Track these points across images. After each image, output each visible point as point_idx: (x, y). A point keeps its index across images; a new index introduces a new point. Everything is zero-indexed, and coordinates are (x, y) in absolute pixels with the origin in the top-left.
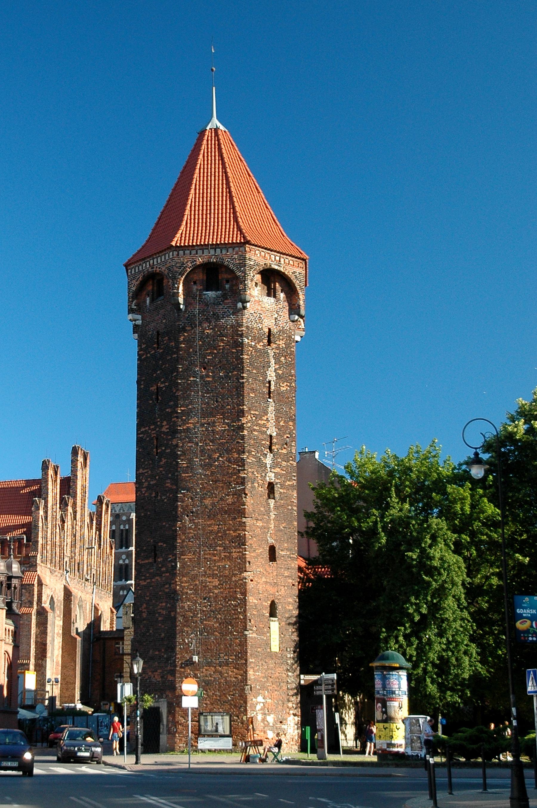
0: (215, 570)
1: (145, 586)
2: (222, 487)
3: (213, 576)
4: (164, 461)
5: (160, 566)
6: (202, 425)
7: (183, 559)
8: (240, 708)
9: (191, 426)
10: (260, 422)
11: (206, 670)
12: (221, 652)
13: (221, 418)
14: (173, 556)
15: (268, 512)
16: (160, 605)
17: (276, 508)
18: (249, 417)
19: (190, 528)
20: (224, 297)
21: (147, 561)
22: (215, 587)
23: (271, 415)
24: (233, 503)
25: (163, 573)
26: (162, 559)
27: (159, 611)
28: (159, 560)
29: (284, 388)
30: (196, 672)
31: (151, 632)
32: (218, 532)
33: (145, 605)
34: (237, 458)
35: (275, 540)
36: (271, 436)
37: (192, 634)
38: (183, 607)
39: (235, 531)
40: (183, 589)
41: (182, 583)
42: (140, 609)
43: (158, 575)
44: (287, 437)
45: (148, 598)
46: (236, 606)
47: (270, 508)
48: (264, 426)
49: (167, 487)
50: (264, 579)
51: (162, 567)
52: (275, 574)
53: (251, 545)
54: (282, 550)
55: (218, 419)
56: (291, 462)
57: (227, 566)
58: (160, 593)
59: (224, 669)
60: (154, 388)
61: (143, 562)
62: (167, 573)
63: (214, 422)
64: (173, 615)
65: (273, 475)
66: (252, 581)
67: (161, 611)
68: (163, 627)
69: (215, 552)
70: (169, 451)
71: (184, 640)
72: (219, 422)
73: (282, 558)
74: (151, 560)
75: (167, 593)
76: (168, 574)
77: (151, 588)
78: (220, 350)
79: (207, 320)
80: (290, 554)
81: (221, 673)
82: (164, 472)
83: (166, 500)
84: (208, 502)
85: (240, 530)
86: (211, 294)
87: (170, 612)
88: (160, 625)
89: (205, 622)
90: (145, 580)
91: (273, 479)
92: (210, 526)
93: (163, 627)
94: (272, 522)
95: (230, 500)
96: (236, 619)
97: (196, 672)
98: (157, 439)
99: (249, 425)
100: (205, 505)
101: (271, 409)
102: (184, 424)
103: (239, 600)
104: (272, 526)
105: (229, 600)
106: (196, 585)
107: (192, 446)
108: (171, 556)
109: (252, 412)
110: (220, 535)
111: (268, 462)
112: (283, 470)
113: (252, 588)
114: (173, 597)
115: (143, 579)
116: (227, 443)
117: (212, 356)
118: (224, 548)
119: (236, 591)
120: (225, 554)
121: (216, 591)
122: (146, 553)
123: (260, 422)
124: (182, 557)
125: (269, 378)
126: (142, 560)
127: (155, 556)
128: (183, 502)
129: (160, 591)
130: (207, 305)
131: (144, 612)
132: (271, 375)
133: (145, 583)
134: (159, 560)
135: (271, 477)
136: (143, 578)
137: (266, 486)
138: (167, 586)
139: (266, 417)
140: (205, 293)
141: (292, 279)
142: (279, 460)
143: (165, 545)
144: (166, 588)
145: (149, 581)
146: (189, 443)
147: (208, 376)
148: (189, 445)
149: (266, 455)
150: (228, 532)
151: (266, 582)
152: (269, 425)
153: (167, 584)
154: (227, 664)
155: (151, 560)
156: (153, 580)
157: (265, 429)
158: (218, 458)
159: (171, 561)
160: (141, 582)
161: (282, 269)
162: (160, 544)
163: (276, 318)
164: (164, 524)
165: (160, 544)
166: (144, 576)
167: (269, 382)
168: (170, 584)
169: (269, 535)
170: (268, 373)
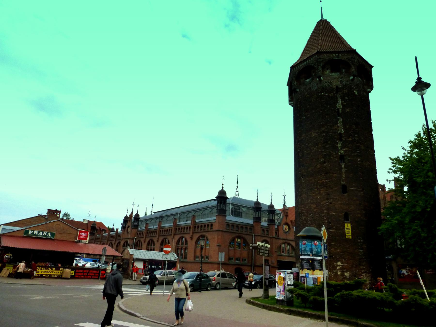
9: (302, 138)
15: (341, 168)
20: (313, 79)
22: (315, 208)
24: (320, 167)
36: (340, 134)
38: (302, 219)
39: (321, 180)
46: (323, 216)
48: (336, 129)
50: (339, 202)
52: (347, 199)
54: (351, 187)
66: (331, 203)
86: (308, 80)
94: (343, 174)
95: (319, 166)
104: (344, 176)
121: (315, 210)
125: (338, 107)
132: (339, 106)
147: (308, 115)
161: (340, 58)
163: (340, 81)
167: (338, 109)
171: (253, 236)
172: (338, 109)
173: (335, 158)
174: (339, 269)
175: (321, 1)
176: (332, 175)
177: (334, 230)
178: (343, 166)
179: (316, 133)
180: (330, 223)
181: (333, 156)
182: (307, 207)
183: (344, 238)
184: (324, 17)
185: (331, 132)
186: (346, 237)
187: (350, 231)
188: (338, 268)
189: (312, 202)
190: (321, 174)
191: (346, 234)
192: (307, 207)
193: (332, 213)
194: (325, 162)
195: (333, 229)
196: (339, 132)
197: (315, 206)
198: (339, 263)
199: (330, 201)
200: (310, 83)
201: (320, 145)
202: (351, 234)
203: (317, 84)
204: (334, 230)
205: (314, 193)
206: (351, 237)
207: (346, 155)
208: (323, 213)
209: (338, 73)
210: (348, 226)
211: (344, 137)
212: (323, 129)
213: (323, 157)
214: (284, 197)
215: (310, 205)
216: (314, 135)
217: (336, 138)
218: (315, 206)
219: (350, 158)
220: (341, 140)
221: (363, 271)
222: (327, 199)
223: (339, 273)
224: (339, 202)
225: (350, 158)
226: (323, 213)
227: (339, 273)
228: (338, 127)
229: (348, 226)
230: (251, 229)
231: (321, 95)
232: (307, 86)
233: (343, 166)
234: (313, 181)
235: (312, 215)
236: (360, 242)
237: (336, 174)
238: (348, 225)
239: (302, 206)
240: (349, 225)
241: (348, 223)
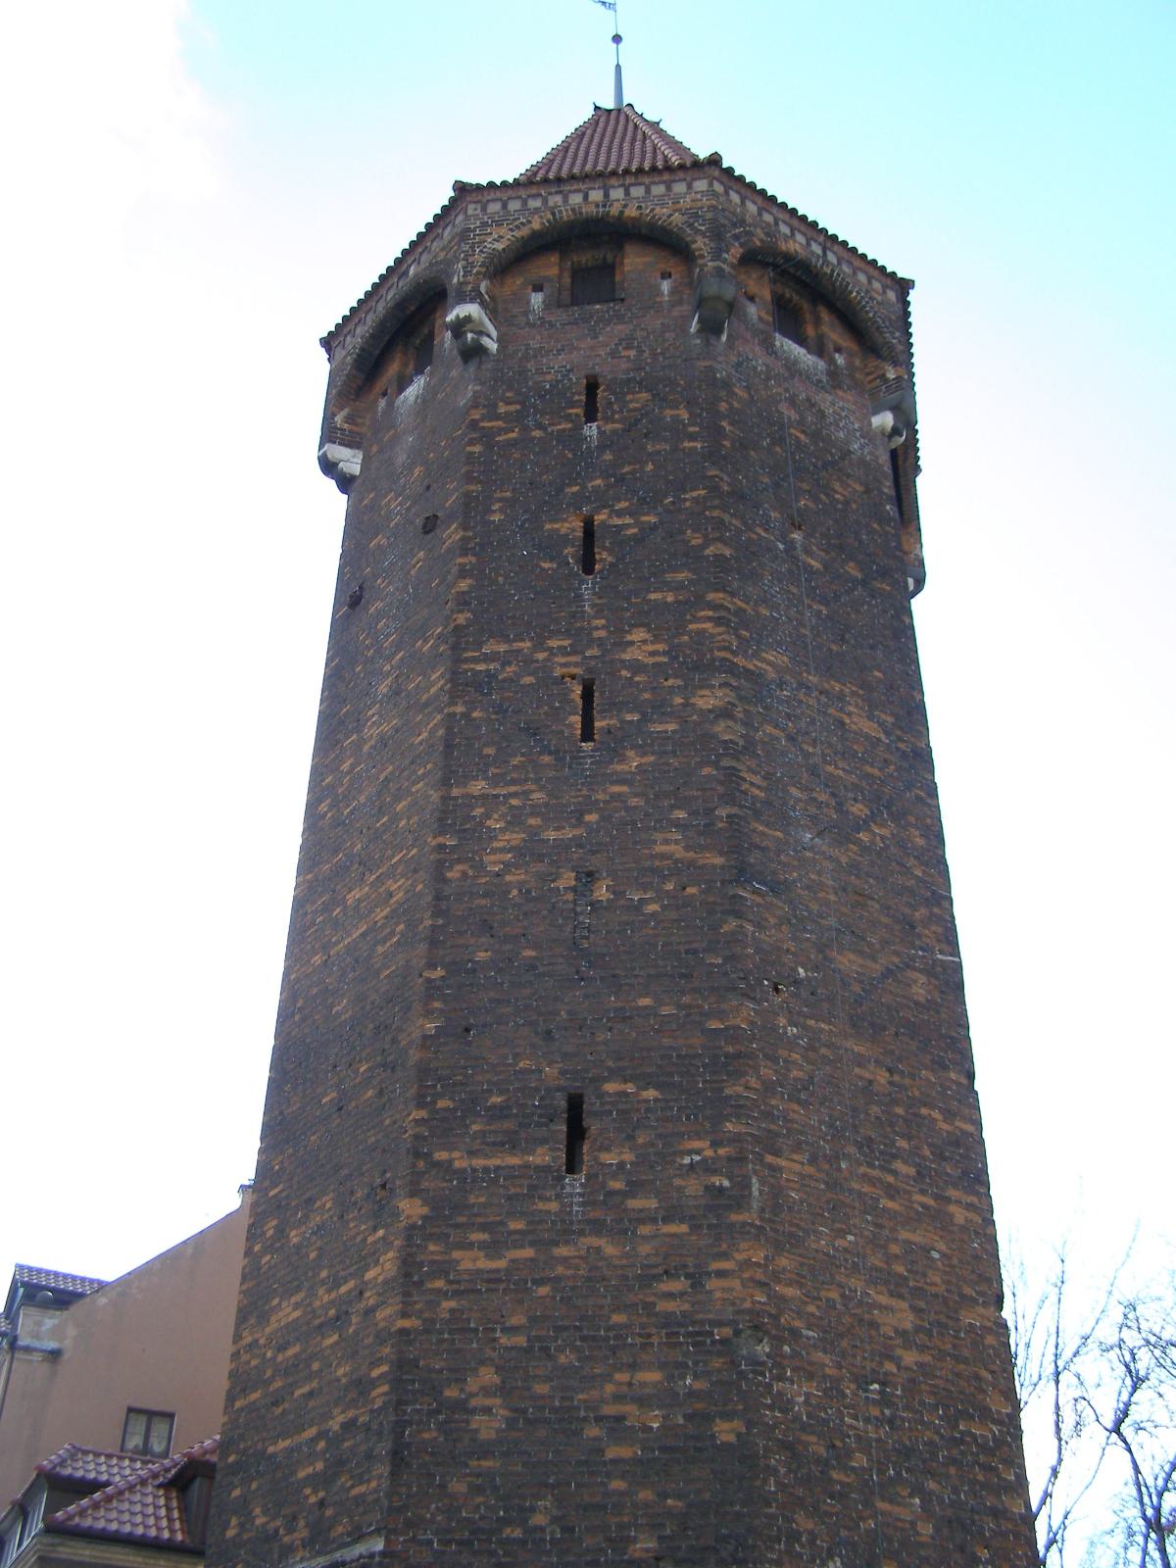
1: (493, 1279)
5: (617, 1185)
14: (715, 1144)
16: (622, 1377)
21: (515, 1161)
25: (642, 1221)
26: (629, 1157)
27: (609, 1410)
28: (610, 1158)
31: (539, 1519)
33: (488, 1376)
38: (783, 1404)
42: (451, 1393)
43: (598, 1227)
45: (521, 1340)
49: (663, 856)
57: (935, 1255)
58: (618, 1318)
60: (572, 526)
61: (479, 1163)
62: (666, 1220)
67: (631, 1409)
68: (645, 1495)
74: (541, 1157)
75: (668, 1321)
76: (684, 1228)
77: (544, 1290)
83: (653, 907)
88: (617, 1484)
90: (493, 1249)
93: (645, 1495)
108: (697, 1144)
114: (724, 1342)
115: (483, 1246)
121: (910, 1358)
122: (508, 1125)
124: (769, 1159)
126: (472, 1153)
127: (576, 1133)
129: (616, 1309)
131: (487, 1410)
133: (502, 1264)
134: (610, 1158)
136: (477, 1236)
143: (651, 1094)
144: (670, 1296)
145: (528, 1253)
150: (924, 1111)
155: (541, 1157)
156: (563, 1251)
159: (708, 1167)
160: (456, 1255)
162: (611, 1087)
164: (645, 1001)
166: (484, 1227)
168: (697, 1279)
189: (876, 1260)
192: (834, 1295)
205: (892, 1192)
235: (885, 1400)
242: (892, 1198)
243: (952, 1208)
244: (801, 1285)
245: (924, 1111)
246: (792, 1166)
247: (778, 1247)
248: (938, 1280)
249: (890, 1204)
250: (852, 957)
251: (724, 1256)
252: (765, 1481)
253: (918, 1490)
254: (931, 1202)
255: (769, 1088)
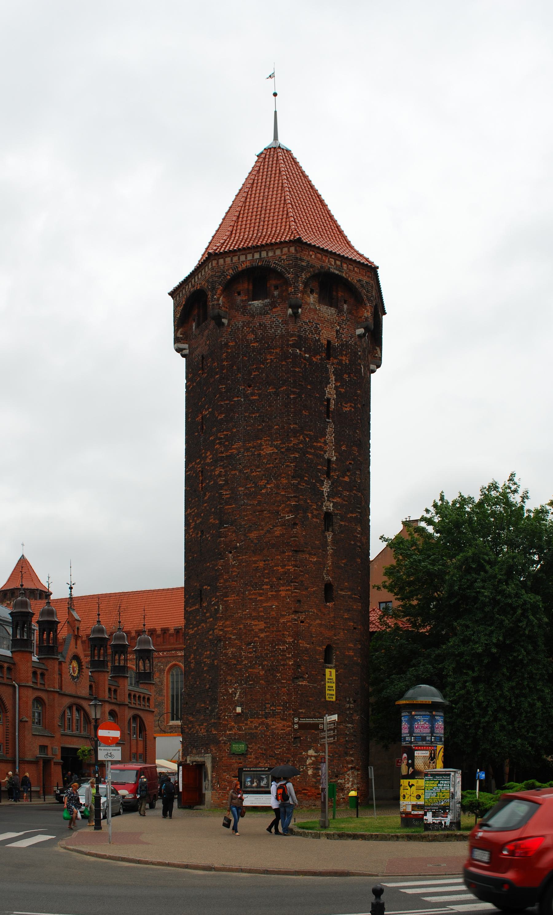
0: (261, 611)
2: (269, 517)
3: (258, 618)
4: (208, 494)
6: (248, 450)
7: (225, 601)
8: (287, 763)
9: (235, 452)
10: (315, 444)
11: (251, 722)
12: (267, 702)
13: (269, 440)
15: (325, 545)
17: (335, 541)
18: (301, 438)
19: (234, 566)
22: (262, 631)
23: (330, 437)
24: (282, 535)
29: (347, 408)
30: (241, 725)
32: (265, 569)
34: (286, 483)
35: (332, 578)
36: (329, 461)
37: (236, 683)
38: (226, 654)
39: (283, 566)
40: (226, 634)
41: (225, 627)
44: (350, 463)
46: (283, 651)
47: (327, 541)
48: (321, 448)
50: (318, 621)
51: (206, 613)
52: (332, 615)
53: (302, 581)
55: (265, 441)
56: (354, 492)
59: (269, 721)
63: (261, 445)
64: (216, 664)
65: (331, 505)
66: (302, 622)
69: (261, 591)
70: (212, 483)
71: (227, 691)
72: (266, 445)
73: (342, 598)
76: (212, 619)
78: (267, 364)
79: (253, 333)
80: (352, 594)
81: (267, 726)
82: (208, 508)
84: (253, 535)
85: (289, 566)
87: (213, 660)
89: (250, 670)
91: (332, 508)
92: (255, 562)
95: (278, 531)
96: (283, 665)
97: (241, 725)
98: (202, 472)
99: (301, 446)
100: (250, 539)
101: (330, 429)
102: (227, 451)
103: (287, 644)
104: (329, 562)
105: (276, 645)
106: (240, 629)
107: (236, 474)
108: (214, 599)
109: (305, 432)
110: (266, 571)
111: (325, 490)
112: (344, 501)
113: (303, 630)
116: (275, 467)
117: (258, 372)
118: (271, 587)
119: (283, 634)
120: (272, 593)
121: (262, 635)
123: (315, 444)
124: (225, 599)
125: (327, 396)
128: (226, 537)
130: (253, 316)
132: (330, 392)
135: (329, 506)
137: (323, 516)
138: (211, 632)
139: (323, 439)
140: (250, 303)
141: (357, 287)
142: (340, 489)
143: (209, 588)
146: (232, 470)
147: (253, 394)
148: (233, 472)
149: (323, 481)
150: (275, 568)
151: (320, 625)
152: (327, 448)
153: (211, 630)
154: (274, 715)
157: (322, 453)
158: (265, 486)
159: (214, 605)
162: (205, 587)
165: (205, 587)
167: (328, 400)
168: (213, 630)
169: (325, 571)
170: (327, 390)
171: (14, 687)
172: (328, 400)
173: (316, 517)
174: (309, 764)
175: (275, 95)
176: (307, 556)
177: (304, 683)
178: (329, 539)
179: (276, 447)
180: (299, 666)
181: (312, 513)
182: (242, 626)
183: (323, 700)
184: (284, 141)
185: (311, 454)
186: (327, 697)
187: (334, 685)
188: (309, 761)
189: (254, 614)
190: (284, 552)
191: (327, 692)
192: (242, 626)
193: (304, 644)
194: (295, 524)
195: (304, 679)
196: (326, 456)
197: (262, 625)
198: (311, 752)
199: (302, 617)
200: (263, 312)
201: (284, 481)
202: (334, 693)
203: (285, 322)
204: (304, 683)
205: (261, 595)
206: (334, 699)
207: (336, 515)
208: (285, 643)
209: (333, 310)
210: (331, 674)
211: (335, 470)
212: (294, 441)
213: (291, 512)
214: (71, 588)
215: (249, 622)
216: (269, 450)
217: (319, 471)
218: (262, 625)
219: (343, 523)
220: (329, 477)
221: (350, 766)
222: (296, 612)
223: (310, 772)
224: (318, 621)
225: (343, 523)
226: (285, 643)
227: (310, 772)
228: (325, 443)
229: (331, 674)
230: (9, 669)
231: (295, 355)
232: (253, 316)
233: (329, 539)
234: (261, 564)
235: (254, 647)
236: (349, 708)
237: (315, 555)
238: (331, 672)
239: (228, 623)
240: (333, 671)
241: (331, 668)
242: (262, 596)
243: (280, 593)
244: (232, 627)
245: (275, 568)
246: (231, 598)
247: (226, 620)
248: (274, 613)
249: (261, 598)
250: (255, 532)
251: (216, 625)
252: (220, 672)
253: (261, 664)
254: (274, 593)
255: (226, 581)
